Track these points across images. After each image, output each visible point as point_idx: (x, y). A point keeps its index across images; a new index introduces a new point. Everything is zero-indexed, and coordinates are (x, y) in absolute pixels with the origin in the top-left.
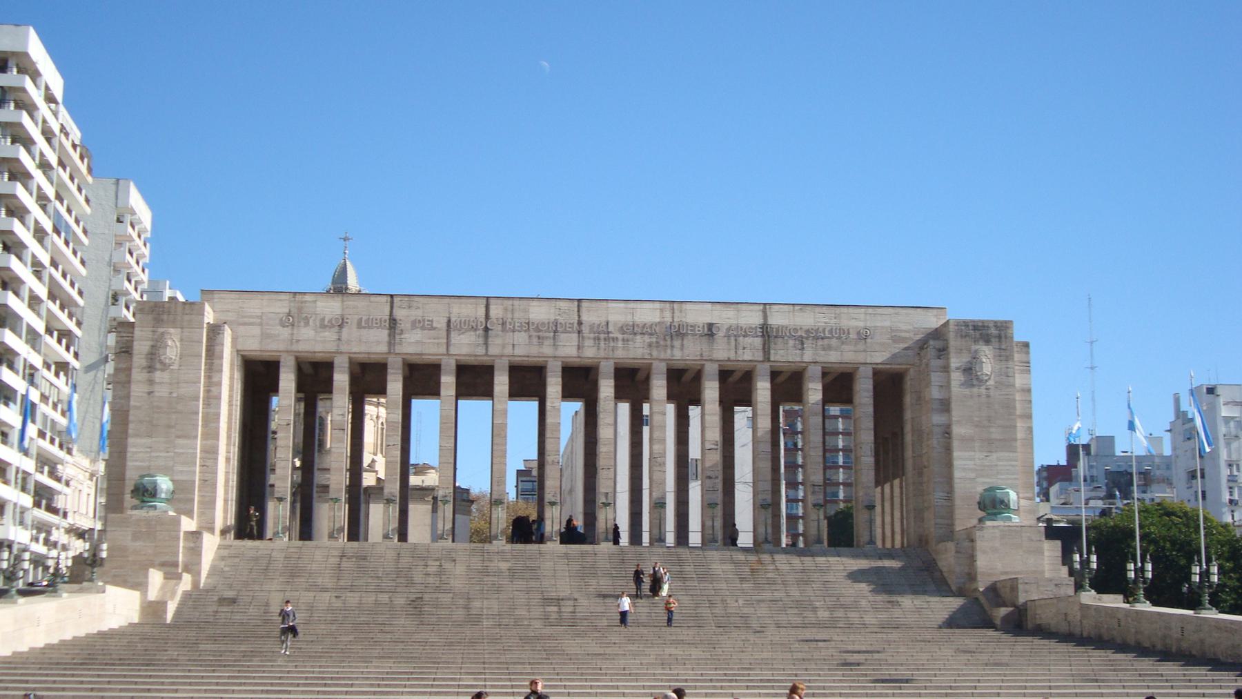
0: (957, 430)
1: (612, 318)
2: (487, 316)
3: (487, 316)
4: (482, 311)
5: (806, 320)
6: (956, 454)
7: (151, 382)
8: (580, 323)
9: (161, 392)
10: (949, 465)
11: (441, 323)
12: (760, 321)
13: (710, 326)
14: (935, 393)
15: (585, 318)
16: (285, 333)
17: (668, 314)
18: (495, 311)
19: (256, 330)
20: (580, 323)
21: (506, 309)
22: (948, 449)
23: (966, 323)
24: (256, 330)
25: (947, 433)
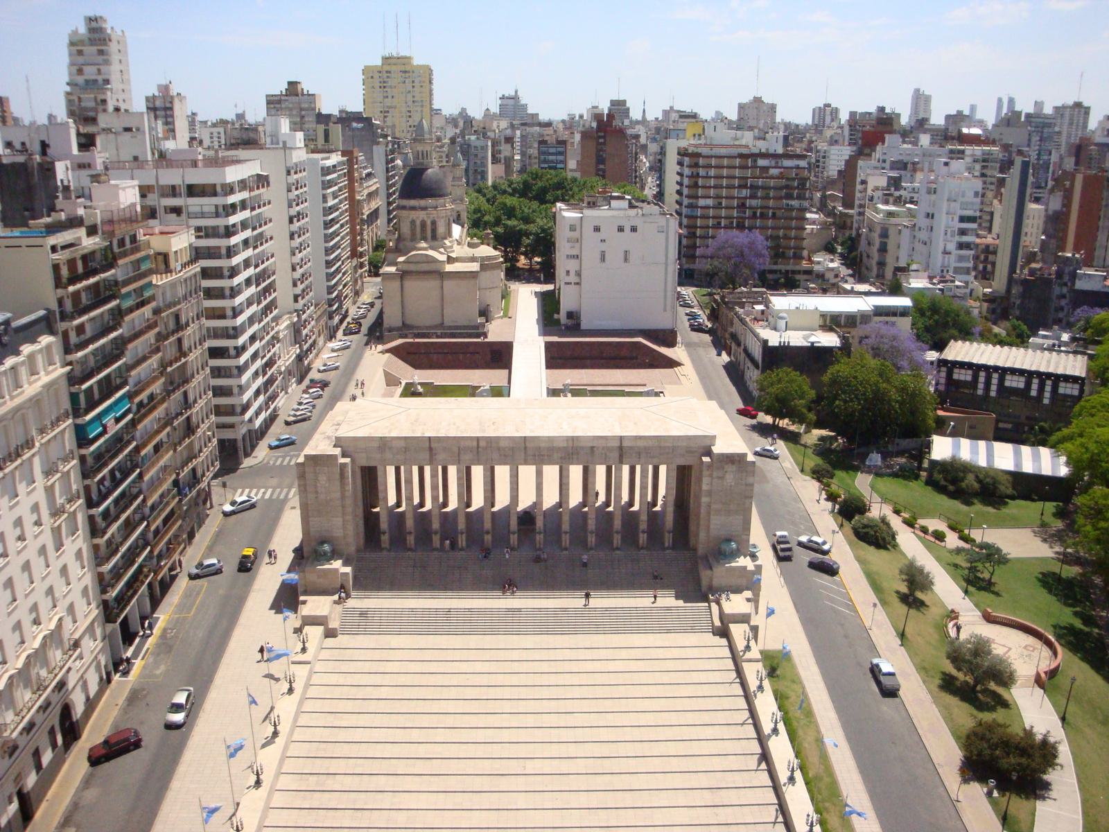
0: (714, 506)
1: (543, 445)
2: (478, 447)
3: (478, 447)
4: (475, 444)
5: (640, 444)
6: (712, 517)
7: (317, 492)
8: (525, 448)
9: (322, 497)
10: (709, 521)
11: (456, 449)
12: (618, 444)
13: (592, 448)
14: (705, 487)
15: (528, 445)
16: (378, 456)
17: (571, 443)
18: (482, 444)
19: (364, 455)
20: (525, 448)
21: (487, 442)
22: (709, 514)
23: (723, 455)
24: (364, 455)
25: (709, 506)
